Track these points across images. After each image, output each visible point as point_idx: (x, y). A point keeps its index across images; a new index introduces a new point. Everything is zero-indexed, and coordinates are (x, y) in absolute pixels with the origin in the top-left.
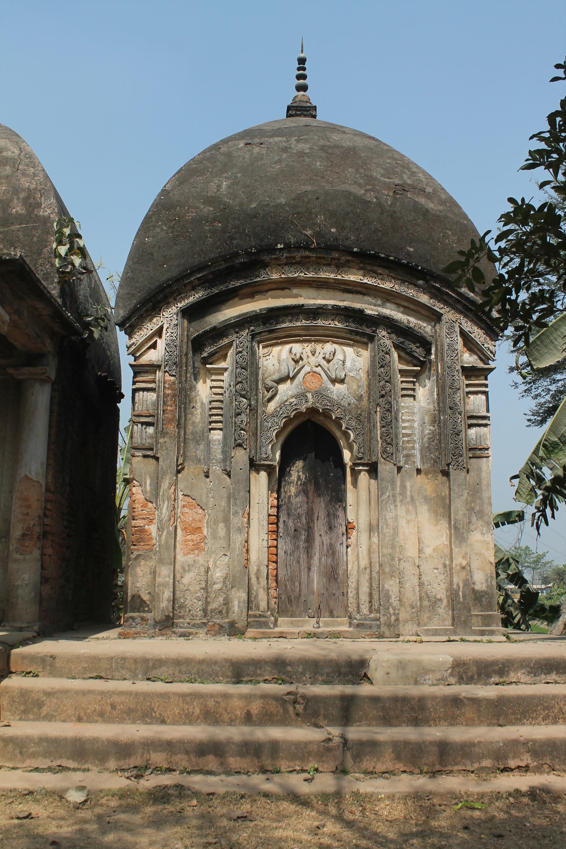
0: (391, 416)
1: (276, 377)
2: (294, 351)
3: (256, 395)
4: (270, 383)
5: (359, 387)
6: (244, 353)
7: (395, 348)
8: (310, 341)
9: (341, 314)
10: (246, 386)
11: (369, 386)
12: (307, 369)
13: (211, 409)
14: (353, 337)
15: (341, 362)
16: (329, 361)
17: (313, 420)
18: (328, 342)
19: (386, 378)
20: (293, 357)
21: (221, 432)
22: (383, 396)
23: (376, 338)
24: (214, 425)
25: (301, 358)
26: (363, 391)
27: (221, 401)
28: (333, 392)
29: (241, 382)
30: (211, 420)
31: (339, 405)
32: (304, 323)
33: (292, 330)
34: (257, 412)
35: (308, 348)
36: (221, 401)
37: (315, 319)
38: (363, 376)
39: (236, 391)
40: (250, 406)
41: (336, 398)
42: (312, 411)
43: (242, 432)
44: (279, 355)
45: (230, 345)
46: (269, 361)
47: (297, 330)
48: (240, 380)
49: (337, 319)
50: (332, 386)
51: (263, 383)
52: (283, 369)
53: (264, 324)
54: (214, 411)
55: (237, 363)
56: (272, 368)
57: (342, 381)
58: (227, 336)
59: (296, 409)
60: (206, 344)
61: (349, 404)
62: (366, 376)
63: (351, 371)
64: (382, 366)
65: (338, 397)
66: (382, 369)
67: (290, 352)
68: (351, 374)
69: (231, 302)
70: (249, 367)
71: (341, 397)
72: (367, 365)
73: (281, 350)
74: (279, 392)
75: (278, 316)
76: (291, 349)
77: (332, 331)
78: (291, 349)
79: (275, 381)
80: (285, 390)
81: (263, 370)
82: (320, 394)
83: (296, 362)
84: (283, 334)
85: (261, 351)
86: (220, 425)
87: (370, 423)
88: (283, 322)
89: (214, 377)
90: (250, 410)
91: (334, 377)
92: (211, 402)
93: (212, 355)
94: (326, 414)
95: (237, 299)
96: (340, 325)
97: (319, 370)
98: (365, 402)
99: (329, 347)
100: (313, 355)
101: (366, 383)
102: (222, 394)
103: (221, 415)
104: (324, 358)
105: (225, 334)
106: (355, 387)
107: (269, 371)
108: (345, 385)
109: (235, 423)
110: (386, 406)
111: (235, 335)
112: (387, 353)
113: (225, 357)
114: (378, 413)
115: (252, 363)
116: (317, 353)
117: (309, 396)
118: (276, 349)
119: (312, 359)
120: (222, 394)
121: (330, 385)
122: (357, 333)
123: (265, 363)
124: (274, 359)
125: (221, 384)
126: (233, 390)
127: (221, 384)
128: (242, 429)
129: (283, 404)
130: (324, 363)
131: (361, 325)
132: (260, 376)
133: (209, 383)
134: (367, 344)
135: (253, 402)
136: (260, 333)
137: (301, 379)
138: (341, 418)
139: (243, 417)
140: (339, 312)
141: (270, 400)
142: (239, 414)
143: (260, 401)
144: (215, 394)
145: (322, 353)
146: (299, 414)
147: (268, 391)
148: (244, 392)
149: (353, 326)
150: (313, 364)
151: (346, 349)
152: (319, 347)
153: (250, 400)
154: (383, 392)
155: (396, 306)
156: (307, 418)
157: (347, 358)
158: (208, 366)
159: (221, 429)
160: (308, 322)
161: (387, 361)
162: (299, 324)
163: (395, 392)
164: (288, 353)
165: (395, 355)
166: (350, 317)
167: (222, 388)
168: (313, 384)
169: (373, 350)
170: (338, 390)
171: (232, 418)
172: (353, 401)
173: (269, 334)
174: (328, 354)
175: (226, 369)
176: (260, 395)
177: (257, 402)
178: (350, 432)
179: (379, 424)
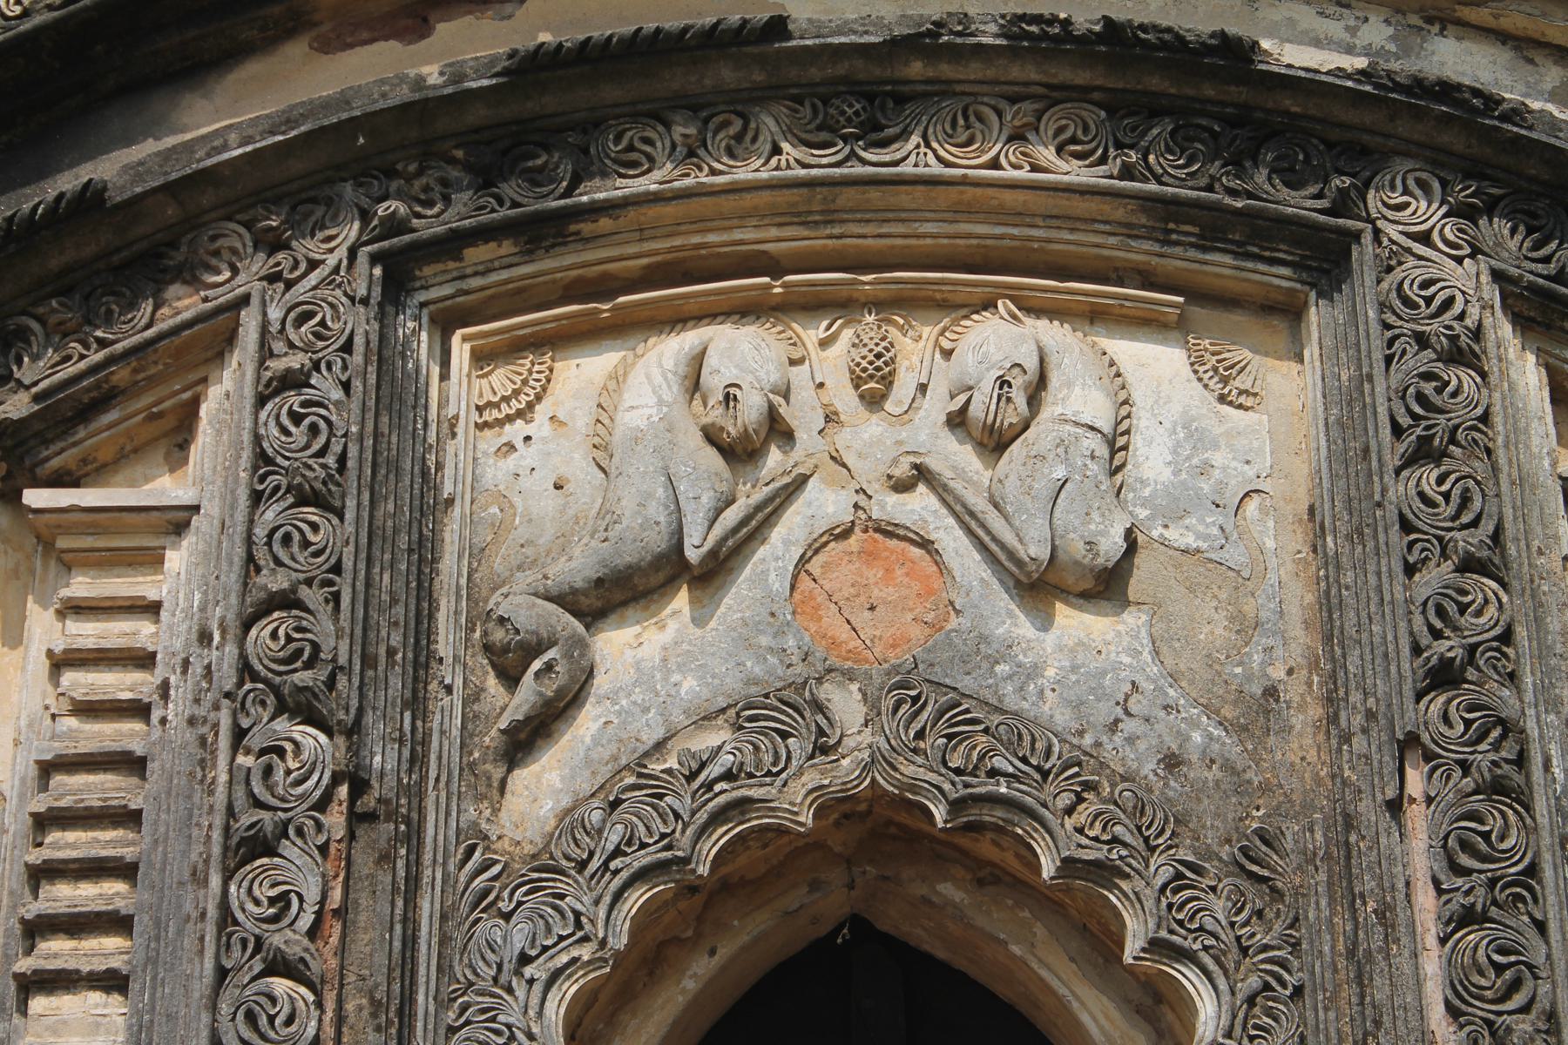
0: (1531, 830)
1: (577, 565)
2: (714, 382)
3: (417, 703)
4: (527, 612)
5: (1246, 627)
6: (325, 386)
7: (1522, 323)
8: (842, 305)
9: (1081, 94)
10: (324, 629)
11: (1328, 606)
12: (824, 503)
13: (43, 822)
14: (1179, 261)
15: (1094, 443)
16: (995, 442)
17: (892, 919)
18: (989, 305)
19: (1467, 542)
20: (715, 415)
21: (111, 1007)
22: (1443, 677)
23: (1364, 254)
24: (58, 951)
25: (777, 429)
26: (1285, 656)
27: (132, 764)
28: (1035, 671)
29: (286, 601)
30: (32, 909)
31: (1083, 775)
32: (795, 160)
33: (702, 223)
34: (413, 838)
35: (829, 355)
36: (132, 764)
37: (874, 133)
38: (1276, 544)
39: (246, 670)
40: (359, 786)
41: (1063, 719)
42: (874, 826)
43: (280, 985)
44: (604, 413)
45: (213, 338)
46: (525, 457)
47: (743, 217)
48: (278, 582)
49: (1049, 125)
50: (1024, 628)
51: (478, 616)
52: (628, 505)
53: (486, 180)
54: (71, 843)
55: (262, 458)
56: (549, 502)
57: (1107, 585)
58: (190, 275)
59: (743, 805)
60: (23, 335)
61: (1172, 762)
62: (1297, 542)
63: (1175, 513)
64: (1423, 453)
65: (1078, 706)
66: (1428, 476)
67: (694, 384)
68: (1179, 536)
69: (253, 68)
70: (359, 502)
71: (1105, 711)
72: (1301, 470)
73: (618, 378)
74: (601, 683)
75: (594, 125)
76: (698, 360)
77: (1019, 216)
78: (698, 360)
79: (566, 600)
80: (650, 669)
81: (472, 521)
82: (920, 696)
83: (739, 452)
84: (631, 255)
85: (458, 382)
86: (106, 950)
87: (1353, 899)
88: (629, 164)
89: (81, 586)
90: (357, 819)
91: (1037, 550)
92: (47, 769)
93: (68, 412)
94: (981, 846)
95: (296, 49)
96: (1074, 172)
97: (919, 507)
98: (1301, 743)
99: (995, 341)
100: (874, 401)
101: (1299, 598)
102: (139, 710)
103: (125, 870)
104: (957, 421)
105: (179, 256)
106: (1214, 630)
107: (522, 533)
108: (1133, 619)
109: (226, 917)
110: (1483, 757)
111: (259, 264)
112: (1458, 355)
113: (178, 431)
114: (1417, 816)
115: (383, 466)
116: (904, 388)
117: (846, 705)
118: (581, 374)
119: (871, 440)
120: (139, 710)
121: (1011, 622)
122: (1214, 227)
123: (496, 472)
124: (562, 440)
125: (141, 632)
126: (225, 658)
127: (141, 632)
128: (280, 966)
129: (634, 779)
130: (957, 458)
131: (1237, 164)
132: (450, 566)
133: (45, 630)
134: (1290, 312)
135: (382, 759)
136: (452, 244)
137: (779, 585)
138: (1105, 872)
139: (300, 870)
140: (1065, 74)
141: (525, 740)
142: (259, 846)
143: (444, 746)
144: (88, 709)
145: (939, 389)
146: (765, 862)
147: (511, 679)
148: (303, 677)
149: (1175, 177)
150: (868, 471)
151: (1129, 350)
152: (914, 346)
153: (354, 731)
154: (1449, 647)
155: (1504, 55)
156: (832, 904)
157: (1143, 422)
158: (35, 497)
159: (112, 982)
160: (827, 156)
161: (1461, 414)
162: (749, 171)
163: (1543, 652)
164: (672, 391)
165: (1525, 375)
166: (1153, 109)
167: (144, 660)
168: (880, 618)
169: (1347, 343)
170: (1067, 660)
171: (199, 879)
172: (1202, 736)
173: (528, 254)
174: (988, 384)
175: (177, 521)
176: (447, 713)
177: (417, 760)
178: (1189, 978)
179: (1425, 899)
